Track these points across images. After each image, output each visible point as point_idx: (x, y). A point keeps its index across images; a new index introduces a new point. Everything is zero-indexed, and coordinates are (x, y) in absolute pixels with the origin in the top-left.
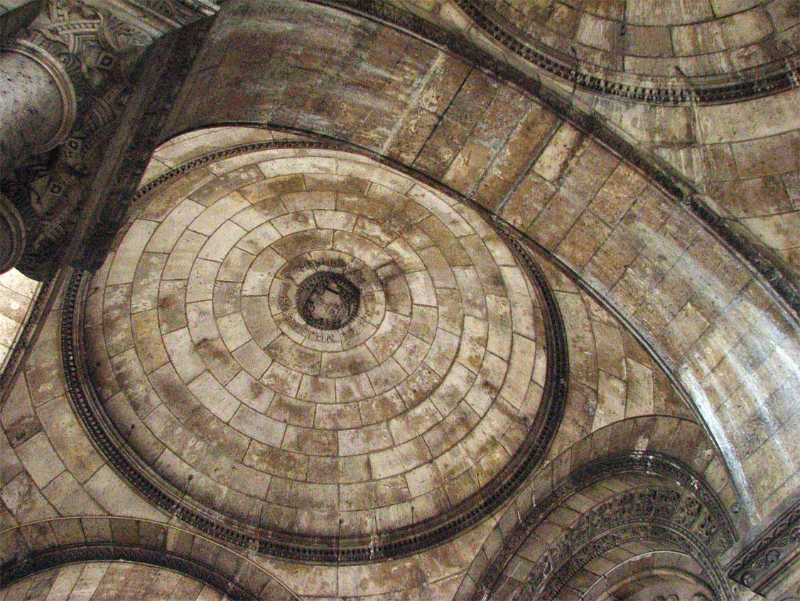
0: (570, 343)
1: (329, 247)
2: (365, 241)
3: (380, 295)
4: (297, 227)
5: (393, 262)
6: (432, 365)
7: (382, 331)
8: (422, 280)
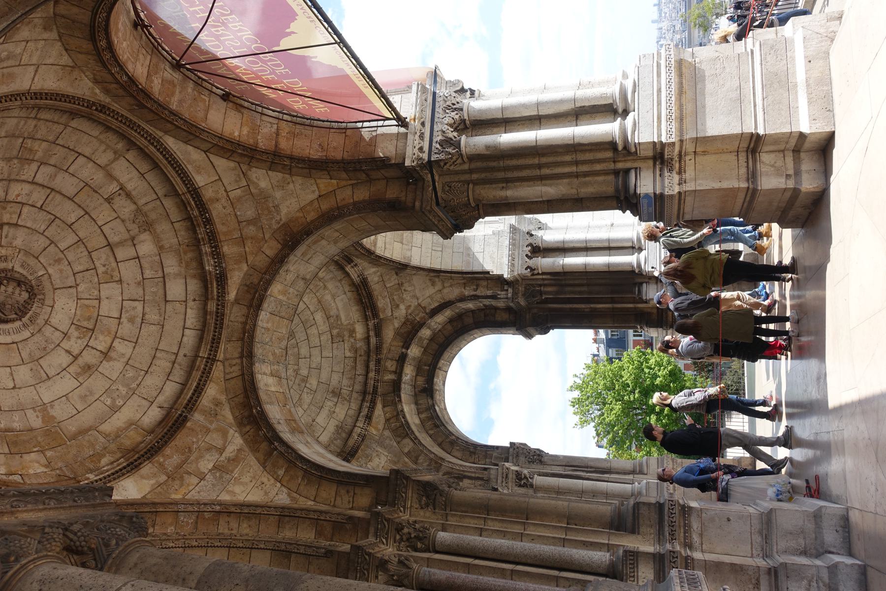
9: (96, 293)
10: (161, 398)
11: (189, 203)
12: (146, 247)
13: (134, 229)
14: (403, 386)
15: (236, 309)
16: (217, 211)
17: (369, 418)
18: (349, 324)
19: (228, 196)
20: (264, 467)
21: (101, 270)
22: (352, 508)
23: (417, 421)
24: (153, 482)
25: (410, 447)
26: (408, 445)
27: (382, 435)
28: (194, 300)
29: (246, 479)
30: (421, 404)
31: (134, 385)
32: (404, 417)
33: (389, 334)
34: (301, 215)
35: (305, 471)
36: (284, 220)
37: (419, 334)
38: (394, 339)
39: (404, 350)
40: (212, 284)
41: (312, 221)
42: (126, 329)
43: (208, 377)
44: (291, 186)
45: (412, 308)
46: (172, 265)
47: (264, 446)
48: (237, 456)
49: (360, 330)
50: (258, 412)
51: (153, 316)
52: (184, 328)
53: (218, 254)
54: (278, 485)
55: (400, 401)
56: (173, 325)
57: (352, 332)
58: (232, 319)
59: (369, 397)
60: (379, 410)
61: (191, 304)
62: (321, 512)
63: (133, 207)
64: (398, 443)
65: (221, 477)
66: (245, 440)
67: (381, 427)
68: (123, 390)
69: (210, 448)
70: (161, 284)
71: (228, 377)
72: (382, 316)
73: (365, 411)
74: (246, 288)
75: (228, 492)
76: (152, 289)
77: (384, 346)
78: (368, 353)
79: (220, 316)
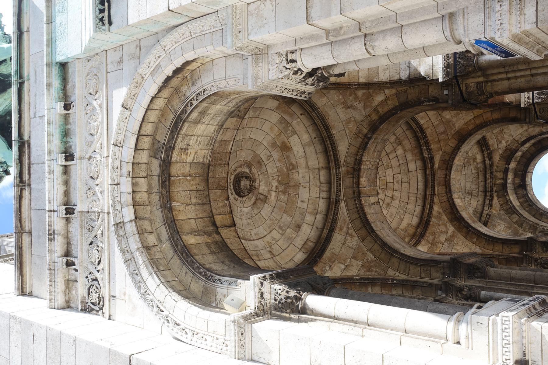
0: (329, 249)
1: (259, 173)
2: (268, 183)
3: (253, 201)
4: (264, 158)
5: (266, 197)
6: (253, 234)
7: (245, 209)
8: (269, 209)
9: (385, 174)
10: (416, 213)
11: (417, 131)
12: (400, 151)
13: (395, 145)
14: (508, 185)
15: (439, 171)
16: (428, 132)
17: (490, 205)
18: (473, 155)
19: (433, 125)
20: (466, 238)
21: (385, 164)
22: (511, 253)
23: (518, 204)
24: (427, 247)
25: (517, 219)
26: (515, 218)
27: (499, 213)
28: (420, 169)
29: (460, 243)
30: (519, 194)
31: (405, 209)
32: (511, 203)
33: (496, 158)
34: (466, 126)
35: (486, 239)
36: (457, 129)
37: (515, 156)
38: (500, 160)
39: (507, 166)
40: (428, 162)
41: (472, 129)
42: (397, 186)
43: (433, 202)
44: (461, 115)
45: (509, 142)
46: (410, 156)
47: (464, 230)
48: (453, 234)
49: (479, 157)
50: (459, 216)
51: (405, 179)
52: (418, 182)
53: (429, 149)
54: (474, 245)
55: (508, 194)
56: (413, 181)
57: (475, 159)
58: (438, 176)
59: (489, 194)
60: (495, 200)
61: (419, 171)
62: (499, 255)
63: (395, 137)
64: (509, 217)
65: (450, 243)
66: (455, 228)
67: (498, 209)
68: (402, 212)
69: (442, 232)
70: (406, 165)
71: (441, 201)
72: (492, 149)
73: (487, 202)
74: (443, 162)
75: (455, 249)
76: (403, 168)
77: (495, 164)
78: (485, 169)
79: (433, 175)
